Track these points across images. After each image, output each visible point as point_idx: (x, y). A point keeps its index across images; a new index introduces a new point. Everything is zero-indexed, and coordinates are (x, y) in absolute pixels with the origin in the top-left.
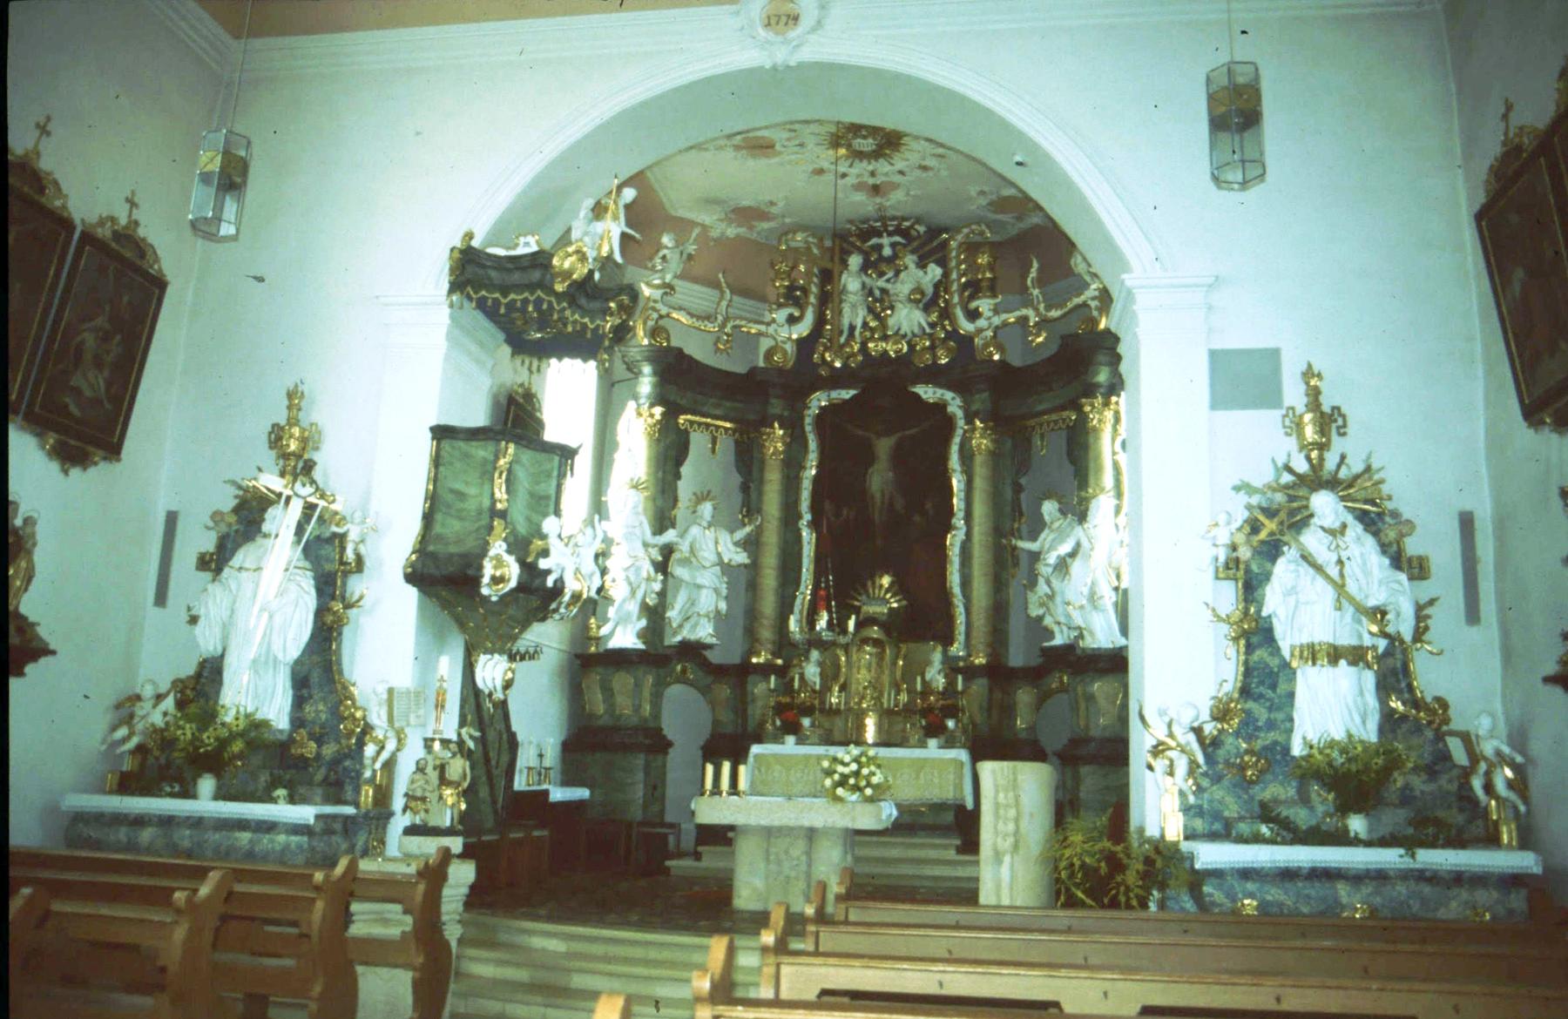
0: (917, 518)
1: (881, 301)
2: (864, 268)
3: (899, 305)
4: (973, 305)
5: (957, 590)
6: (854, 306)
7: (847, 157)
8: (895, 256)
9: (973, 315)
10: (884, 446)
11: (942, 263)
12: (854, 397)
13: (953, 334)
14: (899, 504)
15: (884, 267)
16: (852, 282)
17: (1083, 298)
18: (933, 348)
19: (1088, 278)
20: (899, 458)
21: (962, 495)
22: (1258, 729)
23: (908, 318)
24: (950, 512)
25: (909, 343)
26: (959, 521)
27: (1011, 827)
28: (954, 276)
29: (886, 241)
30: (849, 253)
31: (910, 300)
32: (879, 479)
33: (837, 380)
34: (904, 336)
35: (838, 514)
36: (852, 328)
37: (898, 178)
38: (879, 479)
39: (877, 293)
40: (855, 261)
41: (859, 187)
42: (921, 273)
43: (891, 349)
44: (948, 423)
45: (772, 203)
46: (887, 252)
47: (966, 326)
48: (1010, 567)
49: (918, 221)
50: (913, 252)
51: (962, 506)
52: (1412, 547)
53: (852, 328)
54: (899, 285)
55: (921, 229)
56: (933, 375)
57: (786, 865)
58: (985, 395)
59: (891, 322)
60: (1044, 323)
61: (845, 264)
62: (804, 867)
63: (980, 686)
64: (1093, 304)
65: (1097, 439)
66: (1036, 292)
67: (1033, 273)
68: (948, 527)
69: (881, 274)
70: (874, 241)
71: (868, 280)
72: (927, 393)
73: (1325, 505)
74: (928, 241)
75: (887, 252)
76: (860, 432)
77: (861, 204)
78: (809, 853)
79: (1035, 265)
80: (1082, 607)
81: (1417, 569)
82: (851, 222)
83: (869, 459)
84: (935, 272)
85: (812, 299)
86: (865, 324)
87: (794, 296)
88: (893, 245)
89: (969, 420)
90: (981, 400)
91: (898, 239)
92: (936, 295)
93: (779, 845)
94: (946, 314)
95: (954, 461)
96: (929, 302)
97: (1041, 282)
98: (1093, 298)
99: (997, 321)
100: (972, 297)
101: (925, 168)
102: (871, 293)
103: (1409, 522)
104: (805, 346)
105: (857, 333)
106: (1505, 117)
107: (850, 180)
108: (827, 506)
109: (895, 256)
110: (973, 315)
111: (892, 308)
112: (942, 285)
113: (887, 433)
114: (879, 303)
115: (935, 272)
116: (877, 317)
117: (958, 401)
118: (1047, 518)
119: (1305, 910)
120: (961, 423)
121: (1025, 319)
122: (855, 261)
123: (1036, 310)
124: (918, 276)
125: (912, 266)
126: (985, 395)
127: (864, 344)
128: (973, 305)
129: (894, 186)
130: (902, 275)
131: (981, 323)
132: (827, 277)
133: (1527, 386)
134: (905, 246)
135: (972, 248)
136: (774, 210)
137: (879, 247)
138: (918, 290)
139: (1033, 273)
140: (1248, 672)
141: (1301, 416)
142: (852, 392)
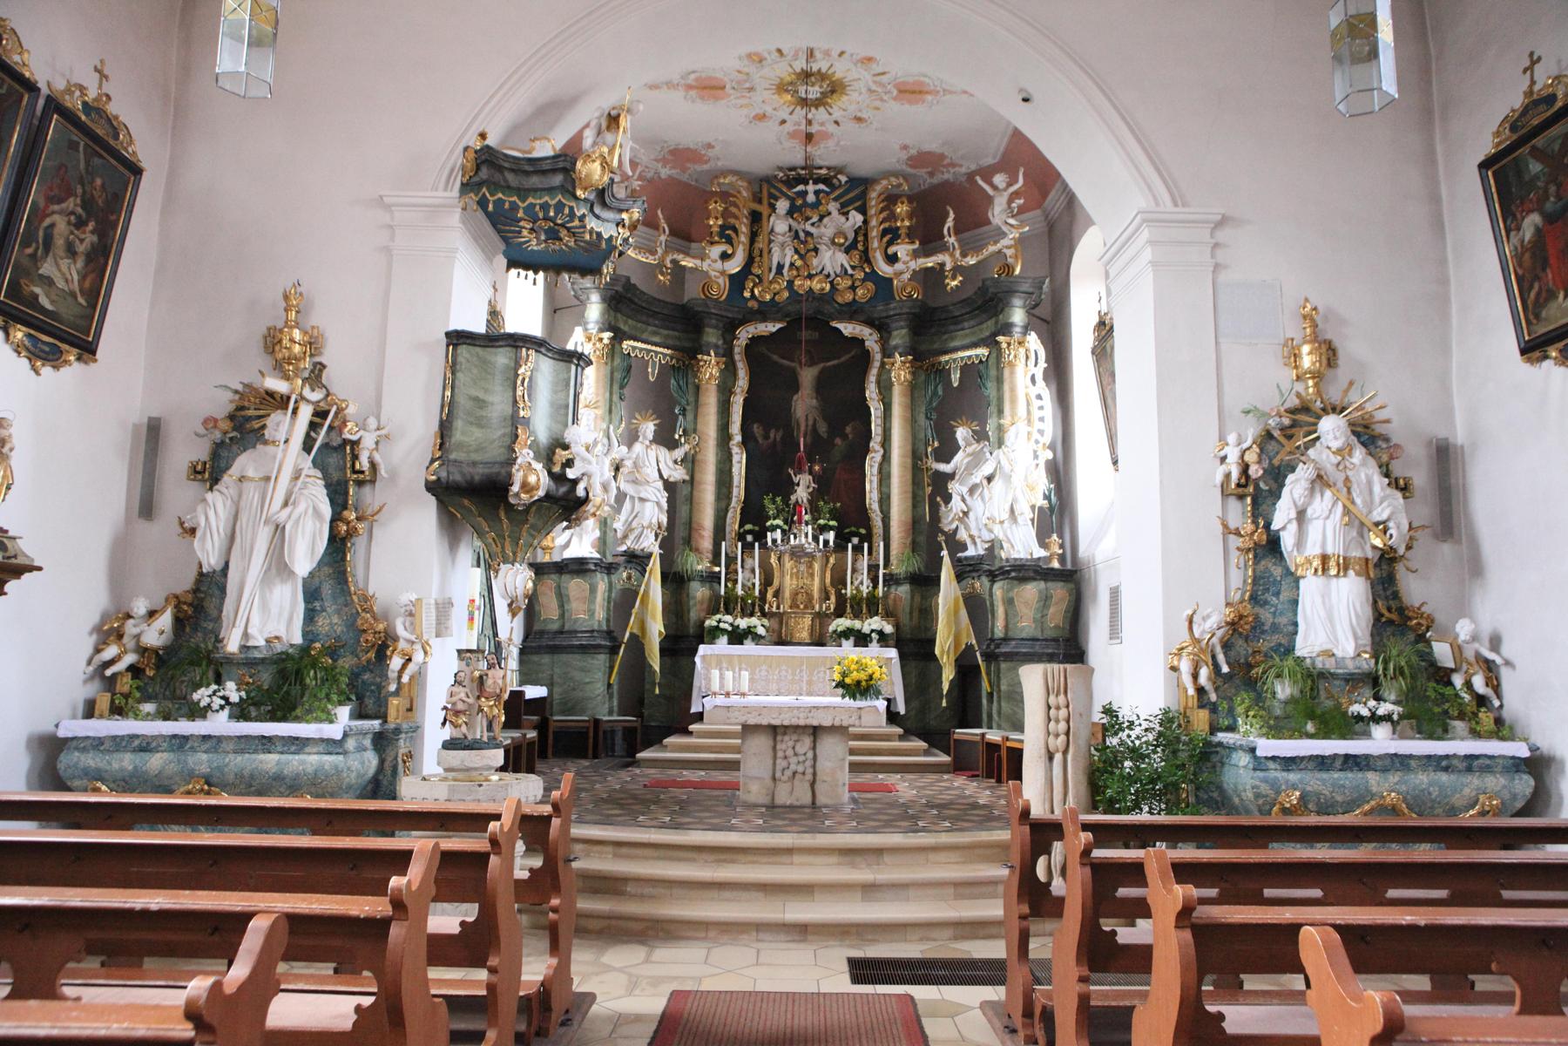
0: (838, 441)
1: (805, 243)
2: (790, 213)
3: (822, 248)
4: (891, 250)
5: (876, 506)
6: (783, 245)
7: (791, 103)
8: (817, 204)
9: (892, 259)
10: (807, 376)
11: (863, 210)
12: (841, 320)
13: (873, 276)
14: (823, 429)
15: (809, 213)
16: (780, 225)
17: (999, 246)
18: (853, 288)
19: (1005, 228)
20: (822, 386)
21: (879, 421)
22: (1263, 632)
23: (831, 260)
24: (868, 436)
25: (831, 283)
26: (875, 444)
27: (1062, 726)
28: (874, 222)
29: (811, 188)
30: (777, 199)
31: (833, 243)
32: (804, 405)
33: (764, 312)
34: (828, 276)
35: (766, 437)
36: (780, 267)
37: (831, 128)
38: (804, 405)
39: (802, 235)
40: (782, 205)
41: (792, 135)
42: (843, 219)
43: (816, 285)
44: (866, 357)
45: (710, 146)
46: (811, 198)
47: (884, 269)
48: (932, 489)
49: (840, 170)
50: (835, 199)
51: (880, 430)
52: (1398, 469)
53: (780, 267)
54: (823, 230)
55: (843, 179)
56: (853, 312)
57: (793, 760)
58: (904, 331)
59: (815, 262)
60: (957, 270)
61: (773, 208)
62: (809, 763)
63: (903, 590)
64: (1009, 252)
65: (1012, 373)
66: (952, 240)
67: (950, 223)
68: (867, 450)
69: (808, 219)
70: (800, 188)
71: (794, 224)
72: (847, 329)
73: (1331, 429)
74: (854, 190)
75: (811, 198)
76: (785, 362)
77: (794, 155)
78: (814, 748)
79: (952, 215)
80: (1002, 522)
81: (1404, 488)
82: (780, 169)
83: (795, 387)
84: (856, 218)
85: (743, 238)
86: (792, 264)
87: (727, 234)
88: (817, 193)
89: (887, 353)
90: (899, 337)
91: (821, 186)
92: (856, 240)
93: (786, 744)
94: (866, 258)
95: (871, 392)
96: (857, 245)
97: (958, 230)
98: (1008, 247)
99: (913, 265)
100: (890, 243)
101: (859, 119)
102: (797, 236)
103: (1397, 446)
104: (737, 281)
105: (785, 271)
106: (1529, 69)
107: (789, 127)
108: (757, 429)
109: (817, 204)
110: (892, 259)
111: (816, 250)
112: (863, 231)
113: (812, 363)
114: (805, 246)
115: (856, 218)
116: (802, 257)
117: (876, 336)
118: (961, 443)
119: (1339, 798)
120: (877, 357)
121: (942, 265)
122: (782, 205)
123: (952, 255)
124: (839, 222)
125: (835, 213)
126: (904, 331)
127: (790, 283)
128: (891, 250)
129: (826, 136)
130: (826, 220)
131: (899, 266)
132: (756, 218)
133: (1528, 322)
134: (828, 194)
135: (891, 199)
136: (711, 153)
137: (804, 194)
138: (840, 233)
139: (950, 223)
140: (1255, 580)
141: (1299, 347)
142: (779, 326)
